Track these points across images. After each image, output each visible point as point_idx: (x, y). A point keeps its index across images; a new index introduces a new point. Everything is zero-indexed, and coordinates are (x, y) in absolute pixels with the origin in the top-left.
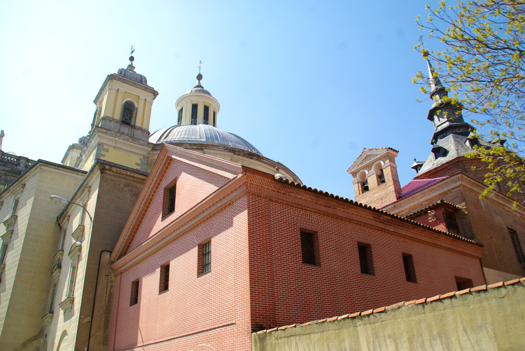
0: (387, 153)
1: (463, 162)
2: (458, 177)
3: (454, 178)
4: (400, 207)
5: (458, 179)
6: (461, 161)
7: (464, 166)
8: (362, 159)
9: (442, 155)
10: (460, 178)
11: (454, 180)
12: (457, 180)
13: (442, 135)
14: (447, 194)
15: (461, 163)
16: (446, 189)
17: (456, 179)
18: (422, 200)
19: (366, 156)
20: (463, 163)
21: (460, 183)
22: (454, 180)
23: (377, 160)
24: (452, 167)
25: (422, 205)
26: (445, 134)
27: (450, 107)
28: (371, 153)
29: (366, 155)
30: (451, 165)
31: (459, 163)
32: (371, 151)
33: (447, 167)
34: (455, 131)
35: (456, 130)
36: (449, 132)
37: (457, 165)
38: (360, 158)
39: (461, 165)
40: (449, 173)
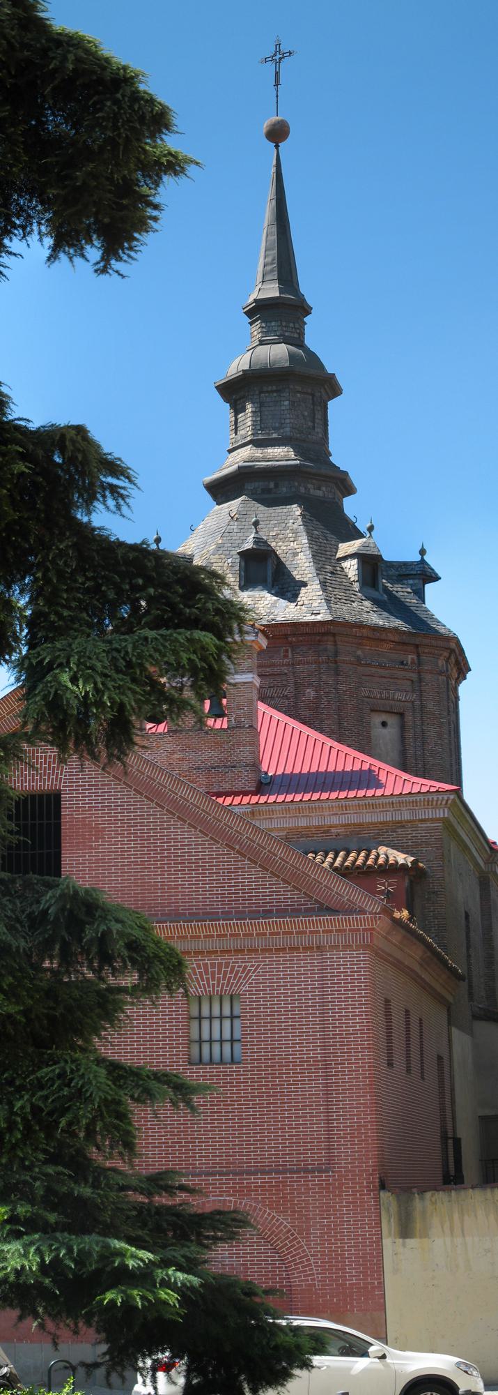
0: (253, 641)
1: (337, 638)
2: (447, 801)
3: (435, 799)
4: (266, 819)
5: (444, 802)
6: (334, 635)
7: (336, 653)
9: (270, 579)
10: (449, 802)
11: (434, 803)
12: (441, 804)
13: (259, 485)
14: (403, 827)
15: (331, 638)
16: (406, 816)
17: (439, 802)
18: (334, 820)
20: (335, 642)
21: (446, 816)
22: (434, 803)
24: (301, 641)
25: (328, 831)
26: (272, 485)
27: (309, 391)
30: (302, 635)
31: (325, 638)
33: (286, 636)
35: (309, 486)
37: (319, 641)
39: (330, 647)
40: (286, 656)
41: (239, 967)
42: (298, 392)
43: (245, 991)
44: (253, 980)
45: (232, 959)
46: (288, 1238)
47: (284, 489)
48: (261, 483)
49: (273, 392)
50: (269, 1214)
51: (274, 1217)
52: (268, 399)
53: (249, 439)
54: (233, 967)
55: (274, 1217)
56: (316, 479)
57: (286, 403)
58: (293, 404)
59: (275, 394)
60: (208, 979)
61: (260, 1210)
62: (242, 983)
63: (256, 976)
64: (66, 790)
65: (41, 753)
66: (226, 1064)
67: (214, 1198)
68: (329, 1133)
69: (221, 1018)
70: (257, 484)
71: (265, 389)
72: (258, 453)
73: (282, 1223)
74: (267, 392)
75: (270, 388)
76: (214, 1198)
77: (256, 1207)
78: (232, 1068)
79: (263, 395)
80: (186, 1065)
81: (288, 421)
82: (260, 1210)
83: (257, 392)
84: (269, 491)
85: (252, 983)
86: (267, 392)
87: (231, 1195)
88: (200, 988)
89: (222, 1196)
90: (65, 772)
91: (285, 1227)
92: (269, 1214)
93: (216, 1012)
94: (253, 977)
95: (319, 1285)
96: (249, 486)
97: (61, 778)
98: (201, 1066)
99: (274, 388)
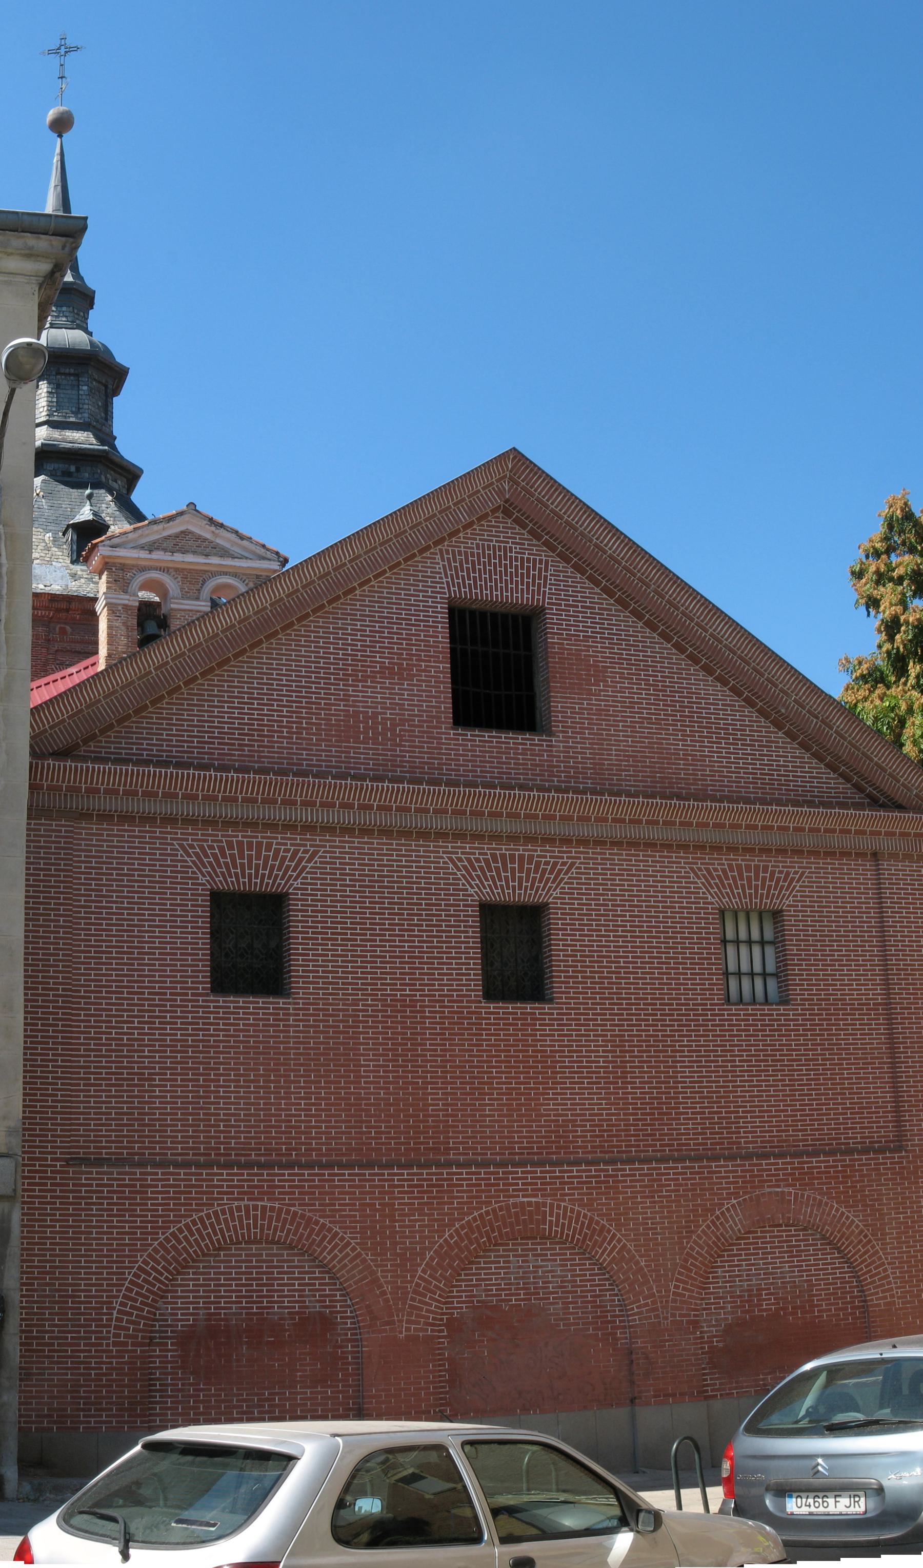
8: (165, 534)
13: (61, 466)
19: (182, 532)
23: (226, 574)
26: (73, 469)
28: (208, 536)
29: (182, 528)
32: (213, 528)
34: (106, 477)
36: (89, 469)
38: (160, 526)
41: (781, 872)
42: (95, 380)
43: (788, 906)
44: (797, 891)
45: (771, 861)
46: (861, 1241)
47: (87, 475)
48: (60, 465)
49: (70, 374)
50: (837, 1210)
51: (843, 1214)
52: (64, 382)
53: (43, 419)
54: (773, 873)
55: (843, 1214)
56: (115, 471)
57: (85, 388)
58: (90, 389)
59: (72, 378)
60: (743, 886)
61: (826, 1204)
62: (784, 895)
63: (800, 886)
64: (552, 609)
65: (516, 553)
66: (772, 1004)
67: (769, 1190)
68: (897, 1100)
69: (750, 942)
70: (56, 466)
71: (62, 370)
72: (56, 434)
73: (853, 1221)
74: (64, 374)
75: (67, 371)
76: (769, 1190)
77: (821, 1201)
78: (764, 1010)
79: (59, 377)
80: (723, 1004)
81: (86, 407)
82: (826, 1204)
83: (54, 373)
84: (70, 474)
85: (796, 896)
86: (64, 374)
87: (789, 1185)
88: (735, 898)
89: (779, 1186)
90: (550, 584)
91: (857, 1226)
92: (837, 1210)
93: (743, 936)
94: (797, 888)
95: (899, 1303)
96: (50, 467)
97: (544, 592)
98: (741, 1007)
99: (72, 371)
